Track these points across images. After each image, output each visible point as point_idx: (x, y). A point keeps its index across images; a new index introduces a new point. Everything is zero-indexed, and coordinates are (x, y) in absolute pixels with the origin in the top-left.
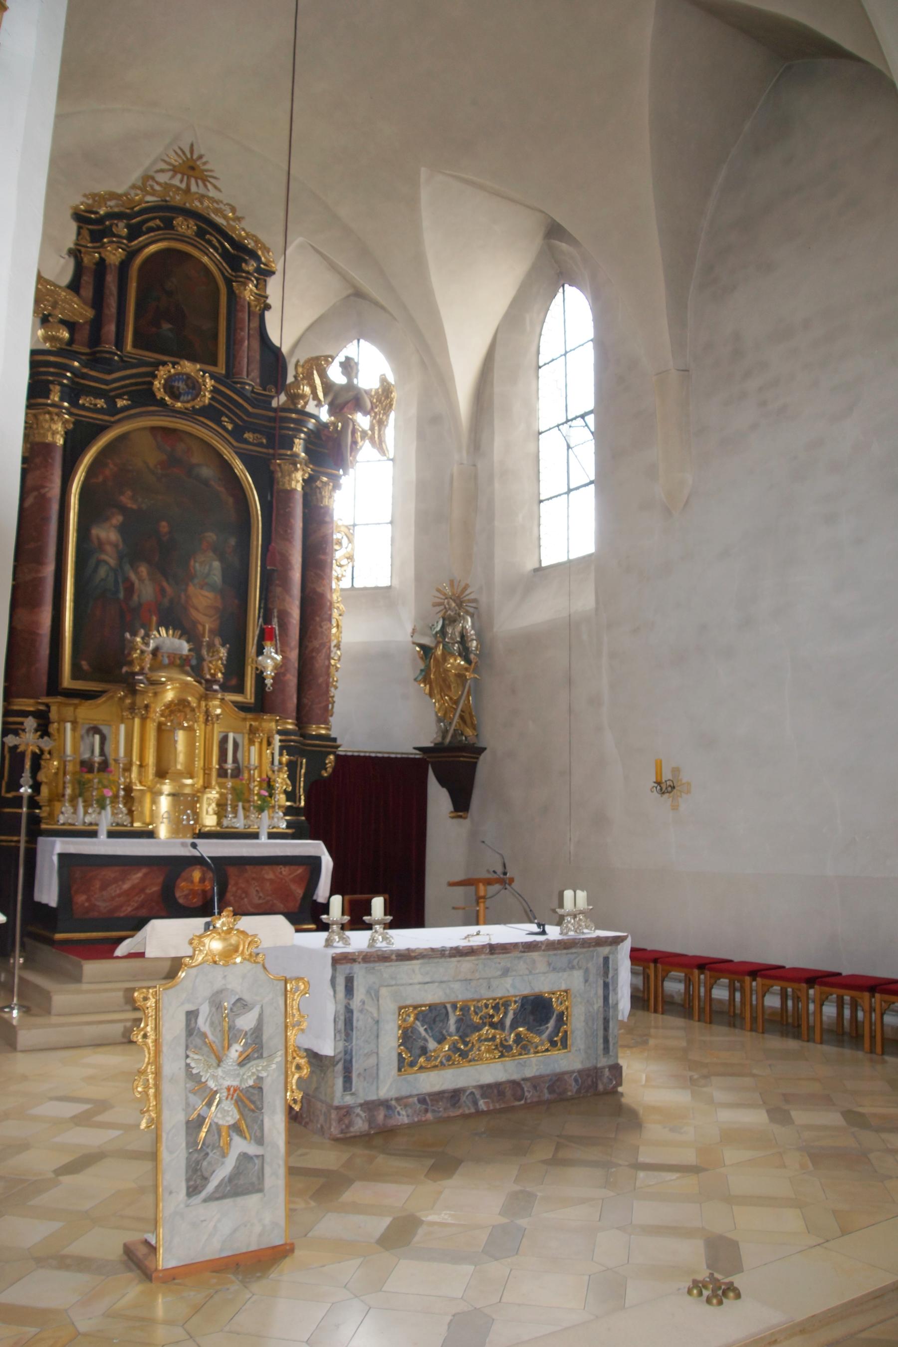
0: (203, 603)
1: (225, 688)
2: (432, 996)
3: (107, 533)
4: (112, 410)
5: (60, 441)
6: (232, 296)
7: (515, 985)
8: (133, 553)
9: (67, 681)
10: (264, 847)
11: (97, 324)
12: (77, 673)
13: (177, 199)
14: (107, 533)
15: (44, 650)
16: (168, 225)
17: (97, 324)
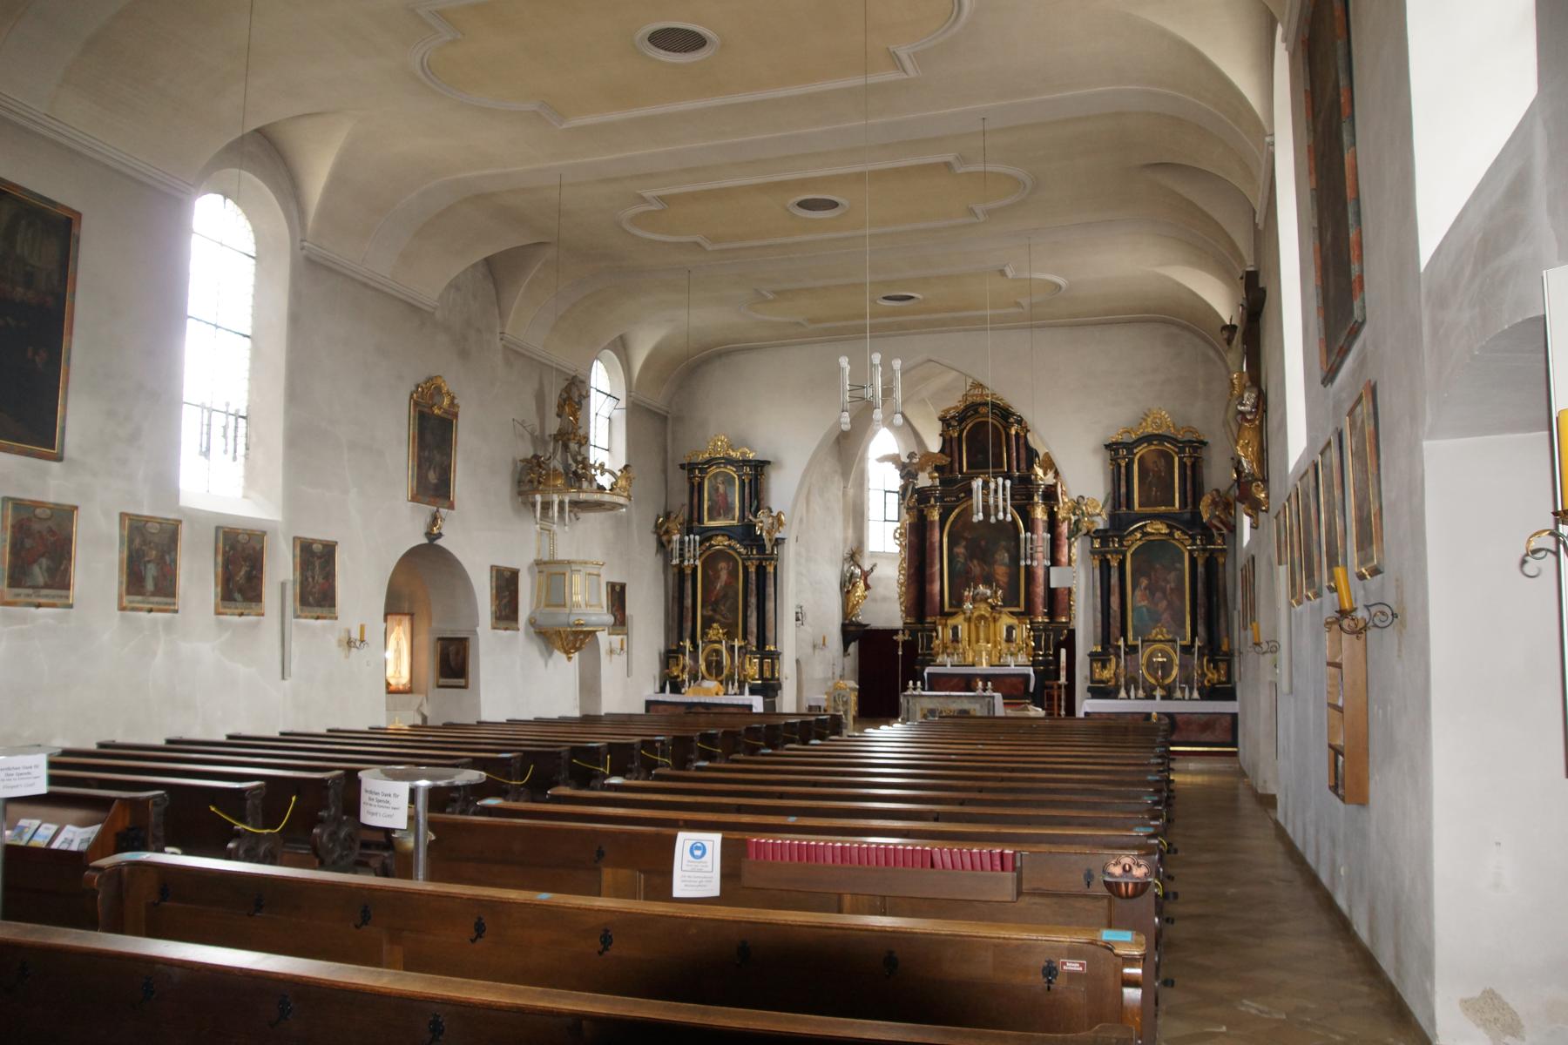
0: (1001, 572)
1: (1004, 606)
2: (931, 706)
3: (960, 550)
4: (958, 499)
5: (937, 518)
6: (1008, 435)
7: (956, 706)
8: (971, 555)
9: (947, 608)
10: (1013, 669)
11: (952, 463)
12: (951, 605)
13: (979, 400)
14: (960, 550)
15: (938, 598)
16: (976, 412)
17: (952, 463)
